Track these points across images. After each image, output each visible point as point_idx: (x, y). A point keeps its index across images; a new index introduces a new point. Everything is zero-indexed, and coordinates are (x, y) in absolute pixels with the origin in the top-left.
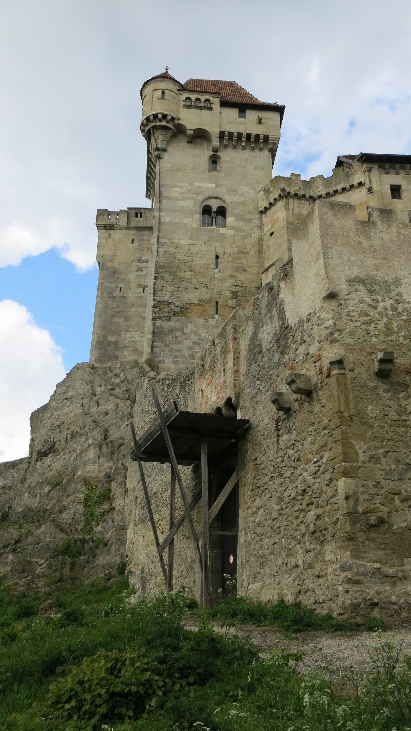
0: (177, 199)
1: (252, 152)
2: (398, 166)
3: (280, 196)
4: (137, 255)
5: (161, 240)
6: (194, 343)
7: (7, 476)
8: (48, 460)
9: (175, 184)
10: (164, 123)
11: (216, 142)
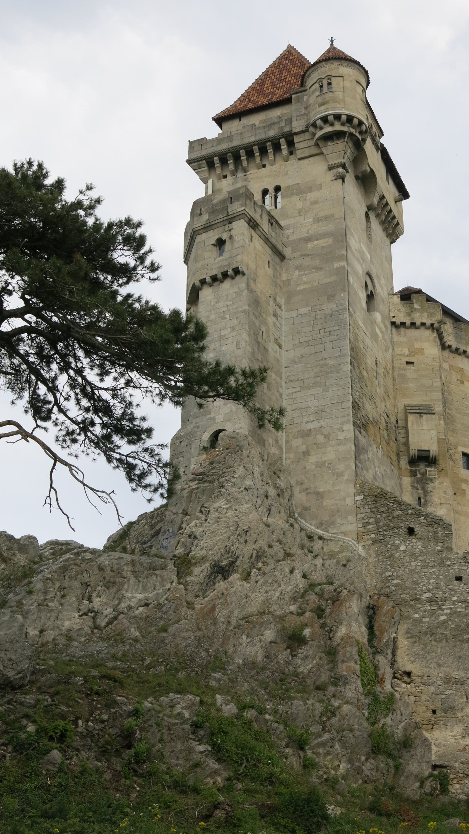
3: (432, 325)
7: (149, 584)
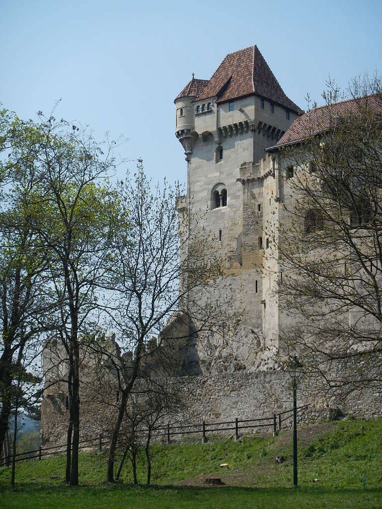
1: (242, 136)
9: (197, 179)
11: (216, 139)
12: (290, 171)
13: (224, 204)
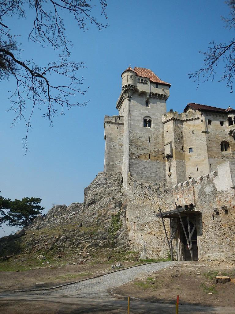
0: (136, 116)
2: (211, 113)
3: (171, 119)
4: (119, 133)
5: (131, 131)
6: (143, 168)
8: (93, 205)
10: (131, 88)
11: (148, 96)
12: (210, 122)
13: (150, 126)
